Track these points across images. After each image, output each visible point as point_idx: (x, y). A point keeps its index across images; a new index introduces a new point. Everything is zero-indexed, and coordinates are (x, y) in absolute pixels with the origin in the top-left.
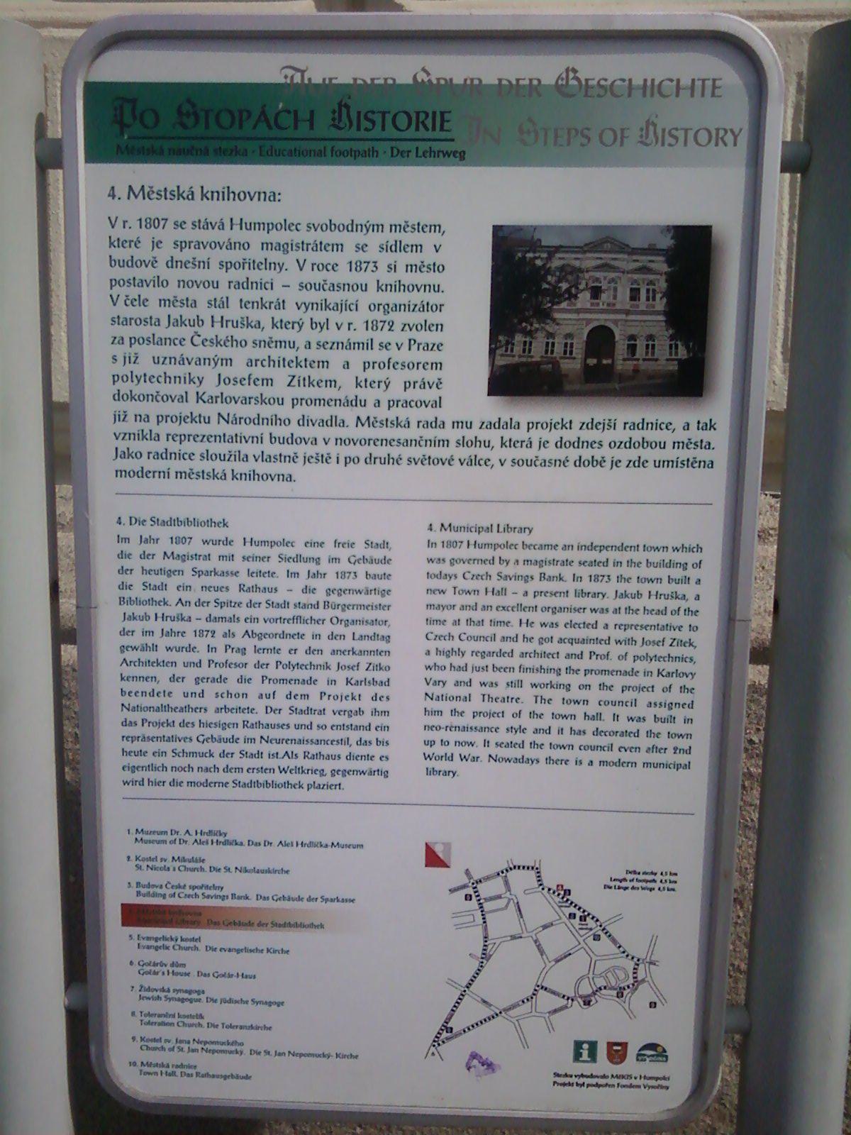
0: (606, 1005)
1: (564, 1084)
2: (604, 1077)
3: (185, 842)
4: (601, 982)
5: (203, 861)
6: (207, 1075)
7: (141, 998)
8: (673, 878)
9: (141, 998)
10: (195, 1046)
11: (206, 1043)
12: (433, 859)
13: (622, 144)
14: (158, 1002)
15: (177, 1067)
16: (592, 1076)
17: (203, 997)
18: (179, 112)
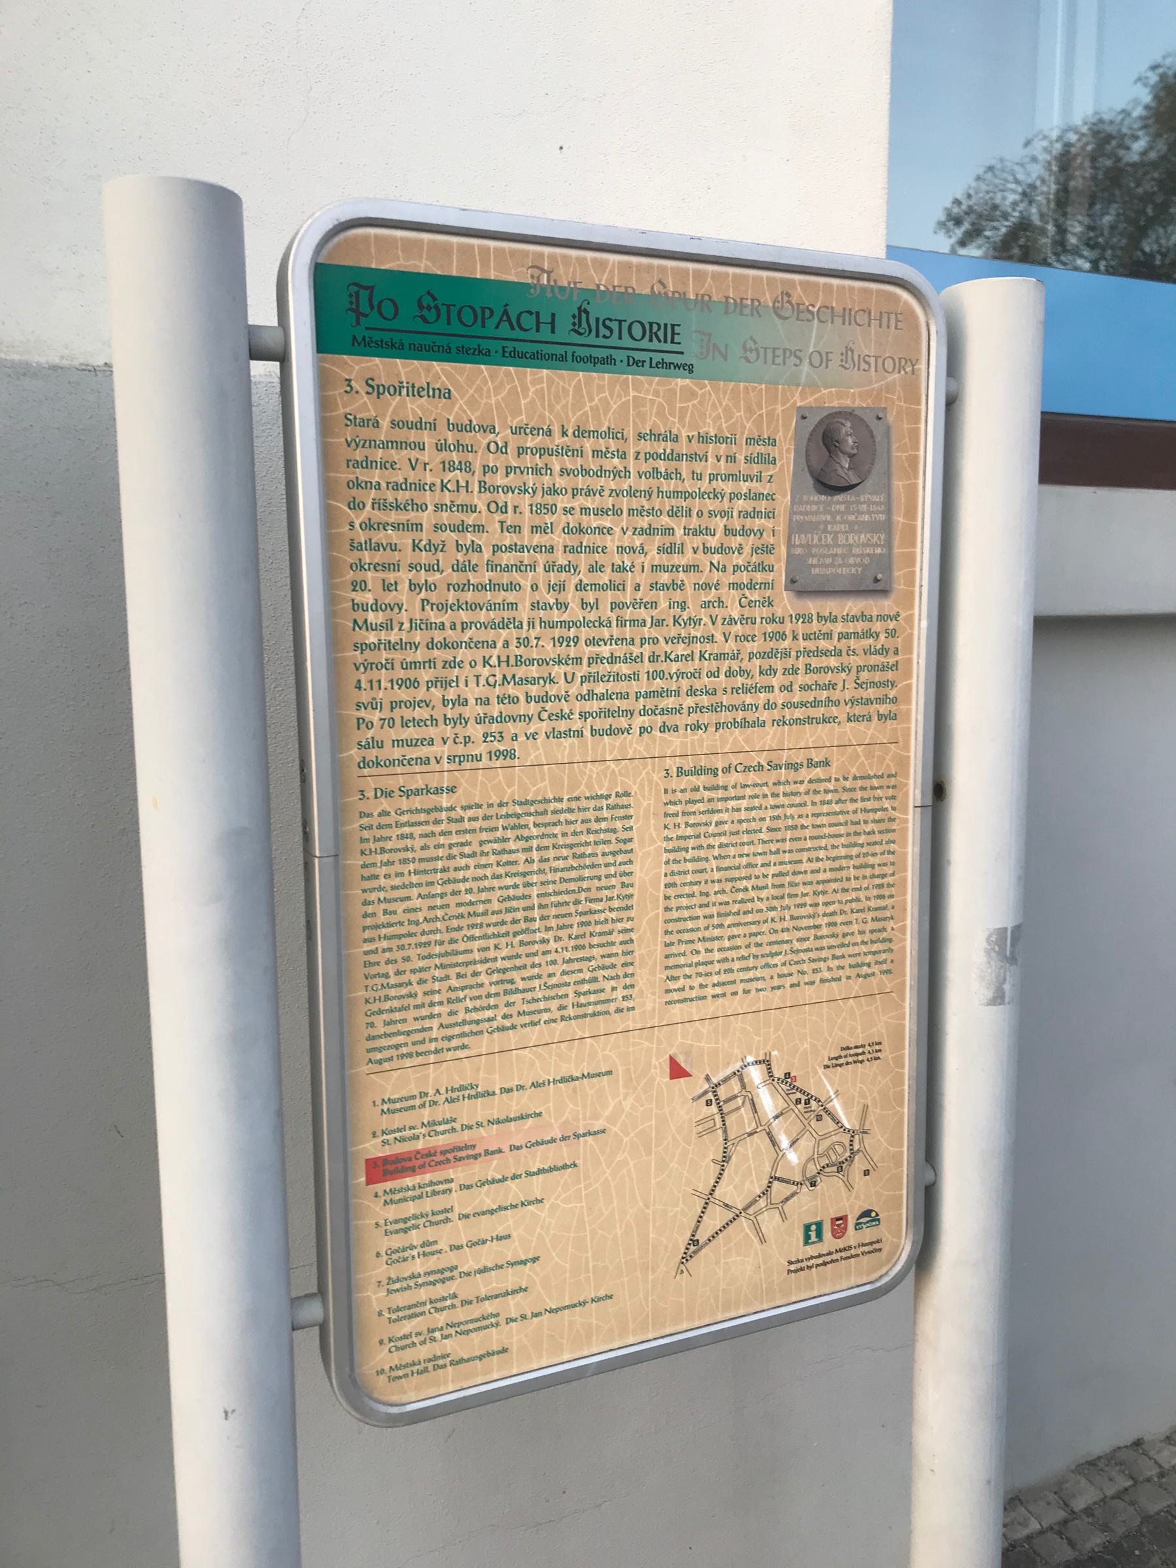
1: (796, 1271)
2: (830, 1253)
3: (435, 1103)
4: (824, 1161)
5: (454, 1120)
6: (462, 1361)
7: (389, 1292)
8: (877, 1047)
9: (389, 1292)
10: (445, 1332)
11: (459, 1324)
12: (677, 1071)
13: (827, 367)
14: (408, 1292)
15: (430, 1360)
16: (820, 1256)
17: (455, 1273)
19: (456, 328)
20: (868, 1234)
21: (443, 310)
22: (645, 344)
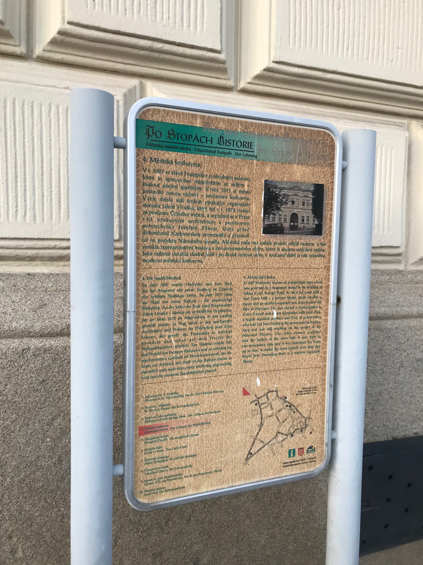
0: (298, 435)
4: (296, 427)
12: (245, 393)
15: (158, 489)
18: (169, 132)
19: (180, 141)
20: (311, 455)
21: (176, 135)
22: (242, 148)
